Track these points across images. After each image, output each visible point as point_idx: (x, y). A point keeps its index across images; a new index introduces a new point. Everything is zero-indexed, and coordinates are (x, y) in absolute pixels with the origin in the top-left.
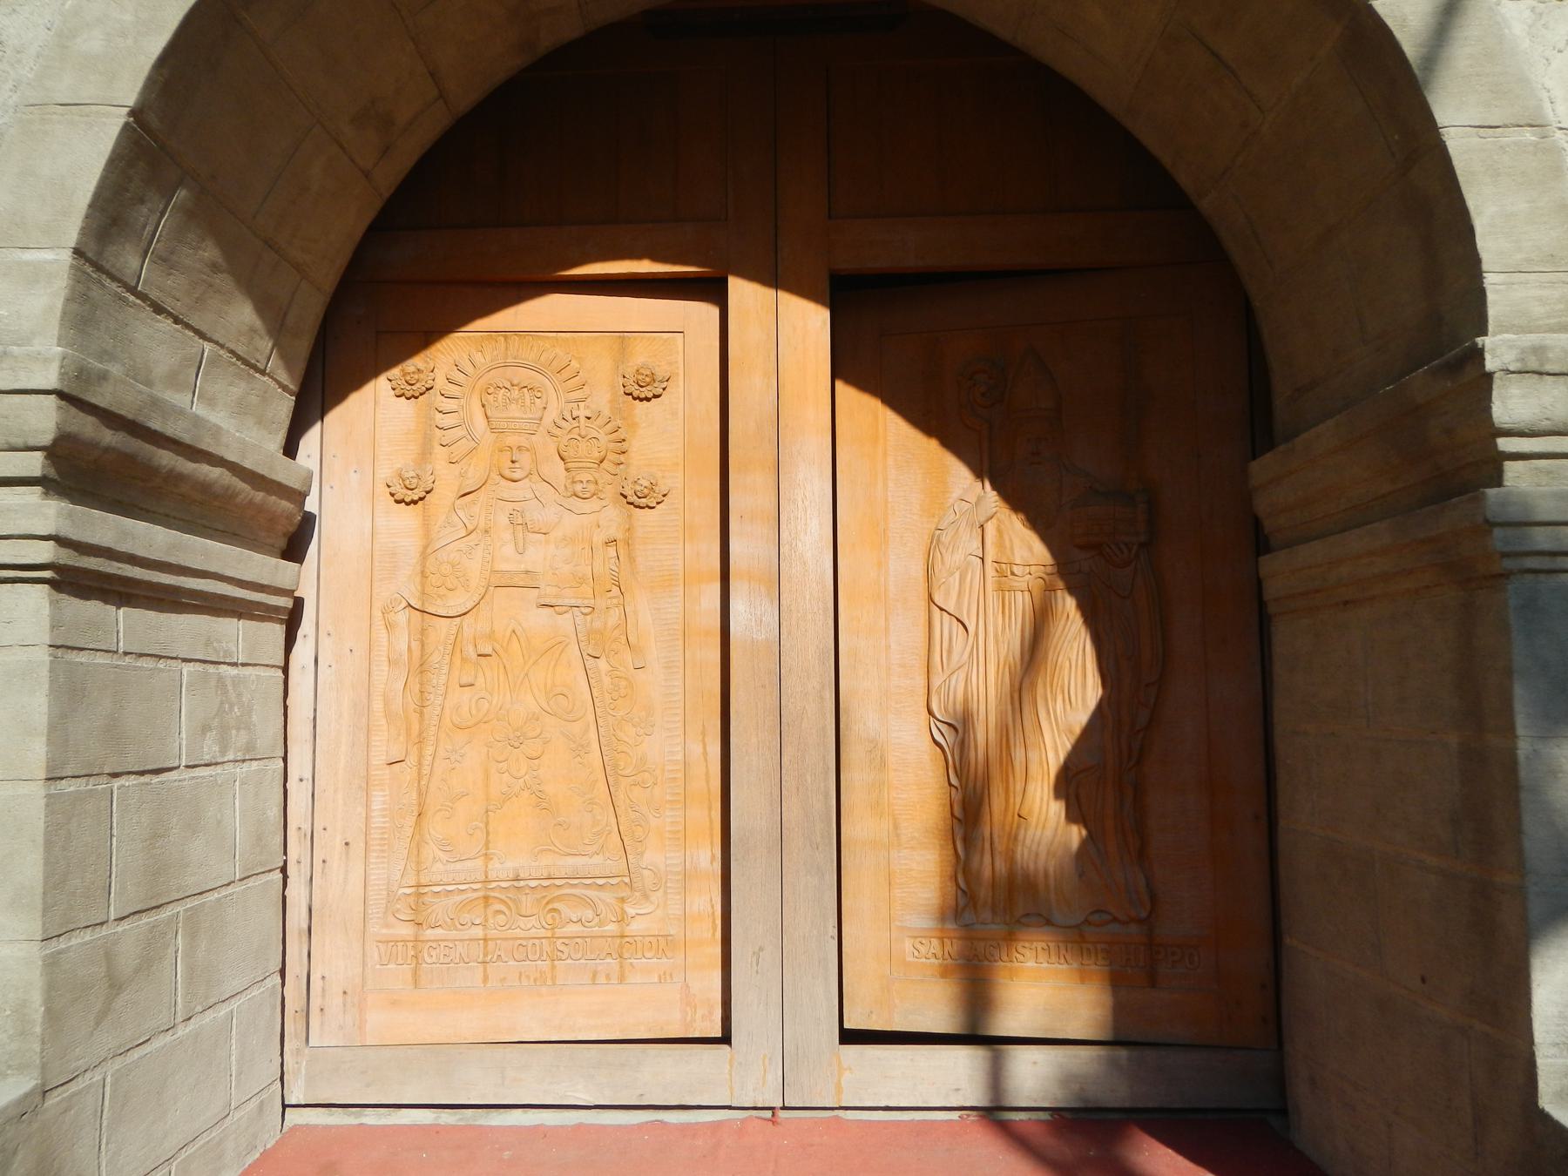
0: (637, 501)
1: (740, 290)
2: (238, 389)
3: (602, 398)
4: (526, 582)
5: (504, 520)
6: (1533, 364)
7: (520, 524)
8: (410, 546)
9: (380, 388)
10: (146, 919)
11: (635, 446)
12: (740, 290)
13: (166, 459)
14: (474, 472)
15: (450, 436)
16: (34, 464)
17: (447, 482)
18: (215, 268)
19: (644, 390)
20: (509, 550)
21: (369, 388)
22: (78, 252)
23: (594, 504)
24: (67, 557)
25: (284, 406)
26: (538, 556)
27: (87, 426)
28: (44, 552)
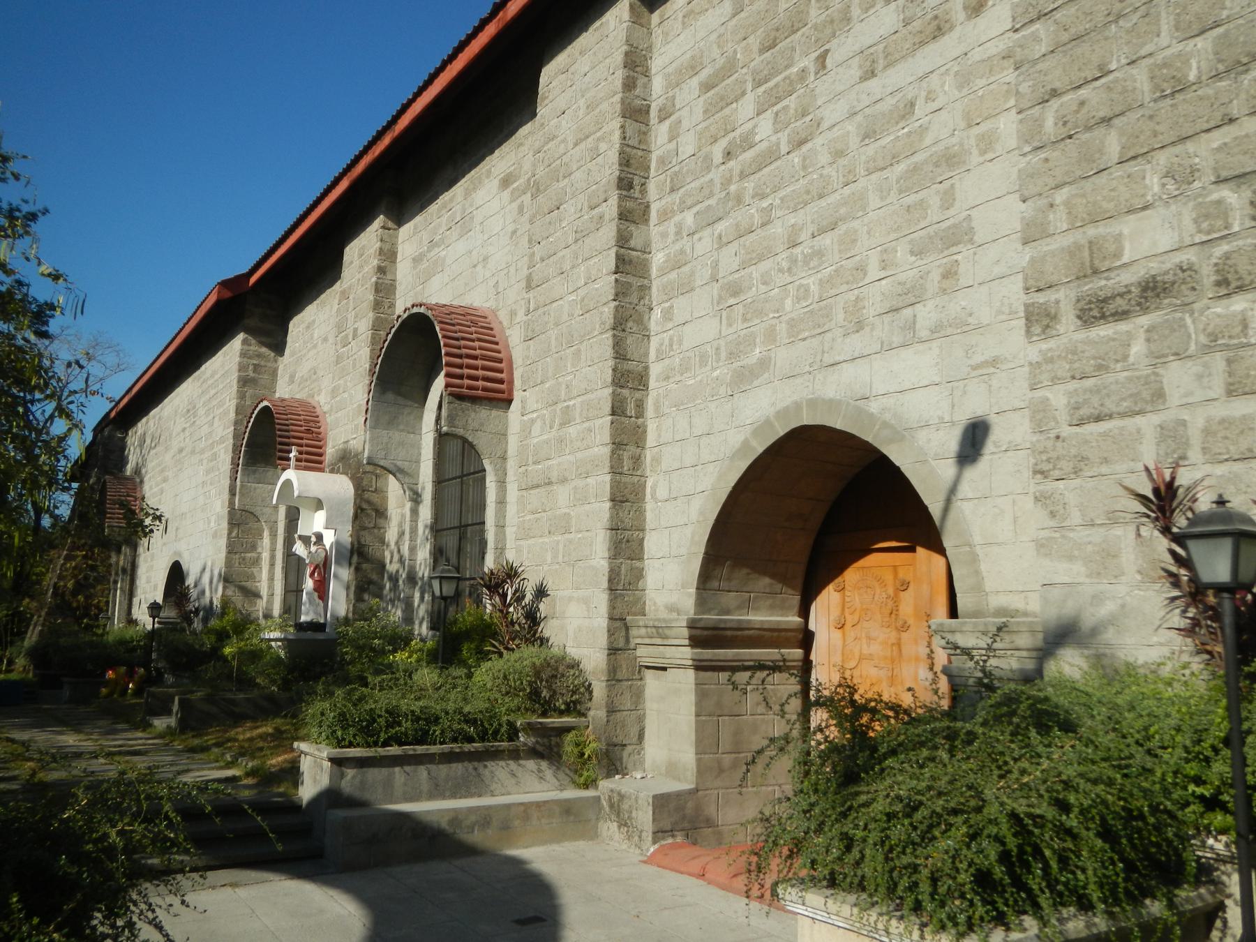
0: (905, 627)
1: (920, 550)
2: (769, 602)
3: (891, 591)
4: (870, 657)
5: (863, 635)
6: (940, 629)
7: (869, 638)
8: (840, 643)
9: (831, 587)
10: (733, 755)
11: (901, 608)
12: (920, 550)
13: (729, 633)
14: (856, 617)
15: (849, 605)
16: (687, 642)
17: (850, 620)
18: (748, 574)
19: (905, 586)
20: (865, 646)
21: (827, 589)
22: (697, 588)
23: (888, 630)
24: (695, 663)
25: (796, 600)
26: (875, 648)
27: (698, 632)
28: (690, 662)
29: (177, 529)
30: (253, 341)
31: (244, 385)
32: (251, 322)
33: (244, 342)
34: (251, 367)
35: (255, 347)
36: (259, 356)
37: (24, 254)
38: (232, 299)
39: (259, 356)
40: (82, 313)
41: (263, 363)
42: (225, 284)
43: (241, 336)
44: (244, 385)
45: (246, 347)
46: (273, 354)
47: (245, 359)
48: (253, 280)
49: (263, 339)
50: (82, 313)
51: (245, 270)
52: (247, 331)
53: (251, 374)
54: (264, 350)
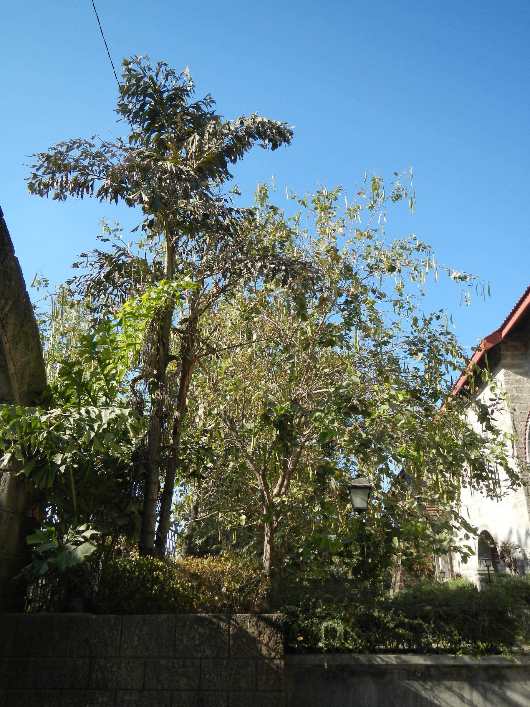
29: (479, 509)
30: (511, 373)
31: (512, 402)
32: (504, 362)
33: (505, 374)
34: (514, 390)
35: (513, 376)
36: (517, 381)
37: (421, 291)
38: (492, 348)
39: (517, 381)
40: (490, 296)
41: (521, 386)
42: (488, 339)
43: (503, 371)
44: (512, 402)
45: (507, 378)
46: (526, 379)
47: (509, 385)
48: (504, 333)
49: (517, 371)
50: (490, 296)
51: (498, 327)
52: (506, 367)
53: (516, 394)
54: (519, 377)
